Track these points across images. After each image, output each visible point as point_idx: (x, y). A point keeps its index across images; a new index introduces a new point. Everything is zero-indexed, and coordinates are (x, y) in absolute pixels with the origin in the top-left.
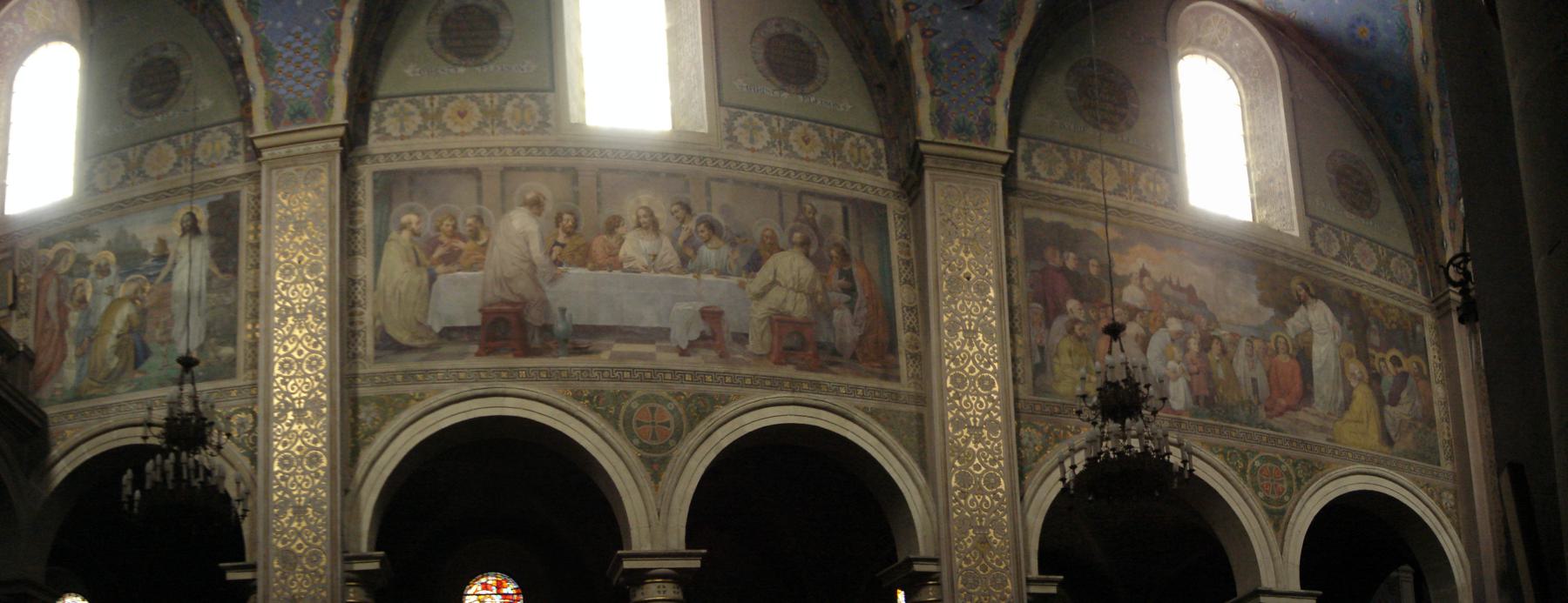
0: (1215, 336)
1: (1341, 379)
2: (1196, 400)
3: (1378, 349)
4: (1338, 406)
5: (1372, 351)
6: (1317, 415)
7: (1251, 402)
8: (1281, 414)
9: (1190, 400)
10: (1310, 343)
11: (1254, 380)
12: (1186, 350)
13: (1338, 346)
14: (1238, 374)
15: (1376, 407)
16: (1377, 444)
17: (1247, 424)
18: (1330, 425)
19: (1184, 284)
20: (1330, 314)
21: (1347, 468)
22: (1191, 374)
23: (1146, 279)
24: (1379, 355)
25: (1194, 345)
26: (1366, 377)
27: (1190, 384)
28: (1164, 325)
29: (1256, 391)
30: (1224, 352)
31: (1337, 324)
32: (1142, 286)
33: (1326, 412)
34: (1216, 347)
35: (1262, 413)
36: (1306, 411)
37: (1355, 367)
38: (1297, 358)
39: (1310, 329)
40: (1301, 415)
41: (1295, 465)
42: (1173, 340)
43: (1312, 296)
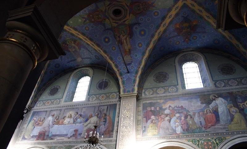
0: (188, 115)
1: (229, 114)
2: (184, 130)
3: (241, 103)
4: (229, 121)
5: (238, 104)
6: (222, 125)
7: (200, 127)
8: (210, 128)
9: (182, 130)
10: (217, 108)
11: (200, 122)
12: (181, 120)
13: (226, 106)
14: (196, 121)
15: (243, 117)
16: (246, 127)
17: (199, 133)
18: (227, 127)
19: (180, 106)
20: (223, 100)
21: (234, 137)
22: (182, 125)
23: (170, 108)
24: (241, 104)
25: (183, 118)
26: (238, 111)
27: (182, 127)
28: (175, 116)
29: (201, 124)
30: (191, 117)
31: (226, 101)
32: (169, 109)
33: (225, 124)
34: (189, 117)
35: (203, 129)
36: (217, 125)
37: (233, 109)
38: (214, 113)
39: (217, 105)
40: (216, 126)
41: (215, 140)
42: (177, 118)
43: (217, 98)
